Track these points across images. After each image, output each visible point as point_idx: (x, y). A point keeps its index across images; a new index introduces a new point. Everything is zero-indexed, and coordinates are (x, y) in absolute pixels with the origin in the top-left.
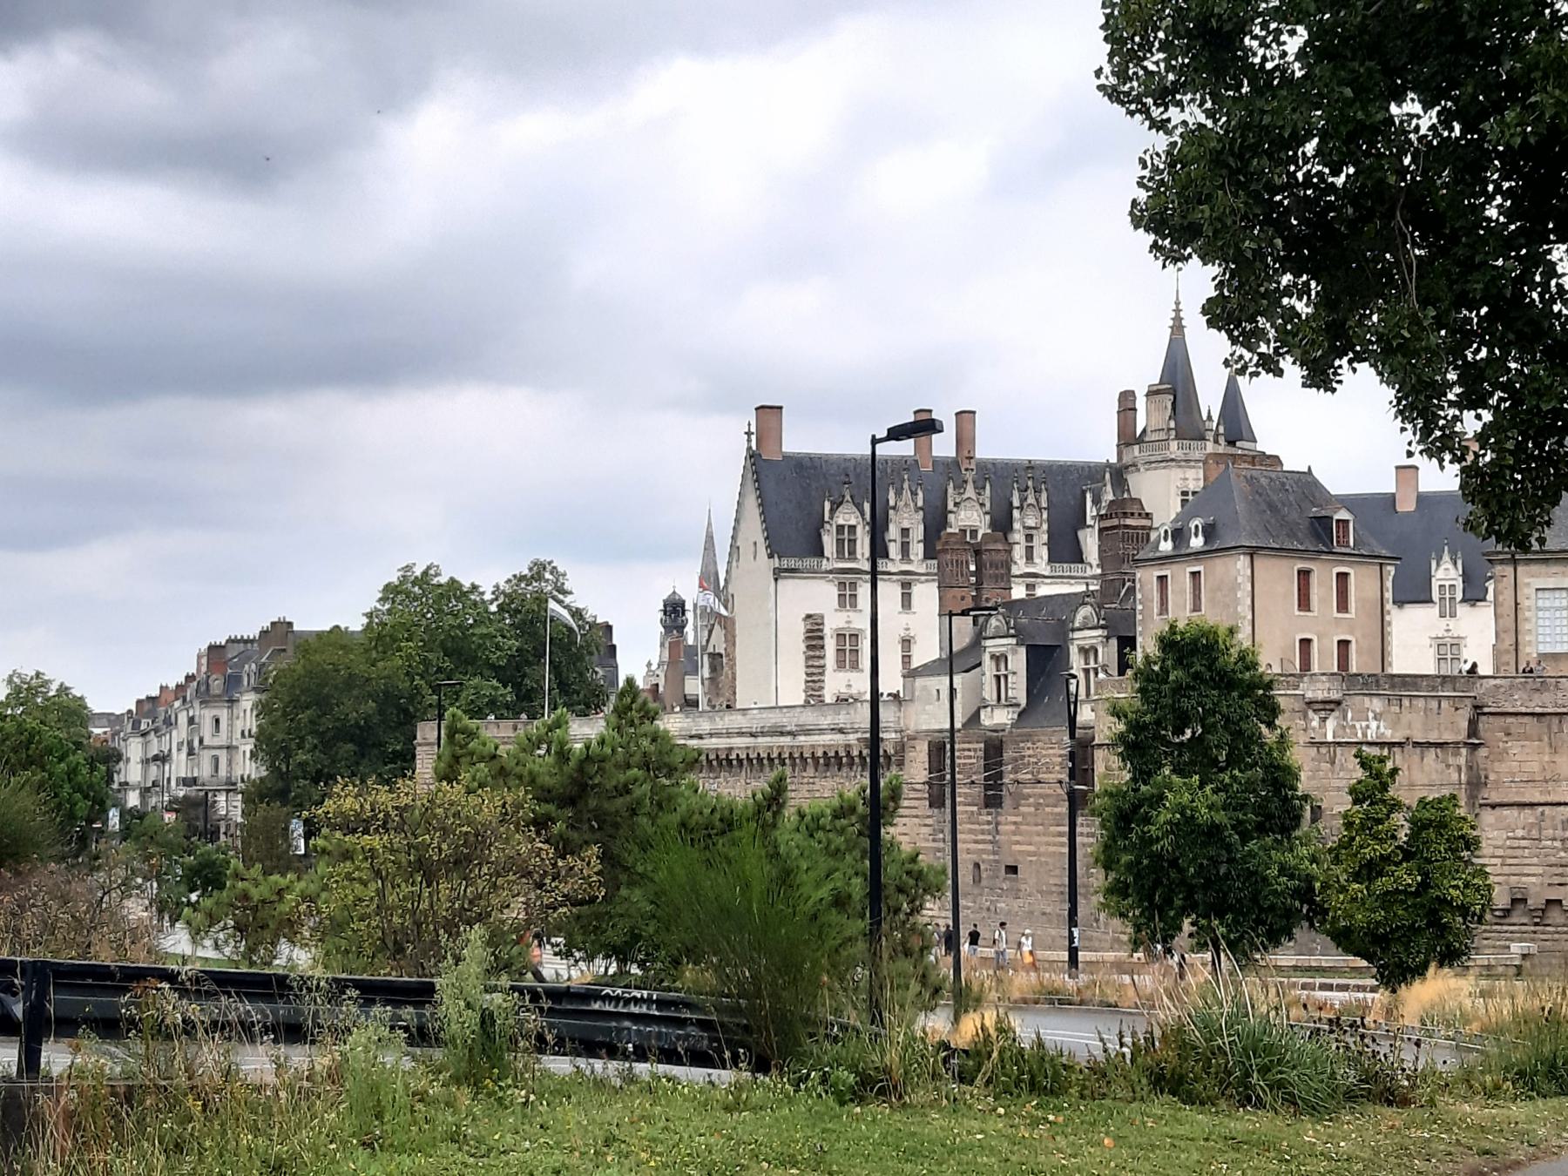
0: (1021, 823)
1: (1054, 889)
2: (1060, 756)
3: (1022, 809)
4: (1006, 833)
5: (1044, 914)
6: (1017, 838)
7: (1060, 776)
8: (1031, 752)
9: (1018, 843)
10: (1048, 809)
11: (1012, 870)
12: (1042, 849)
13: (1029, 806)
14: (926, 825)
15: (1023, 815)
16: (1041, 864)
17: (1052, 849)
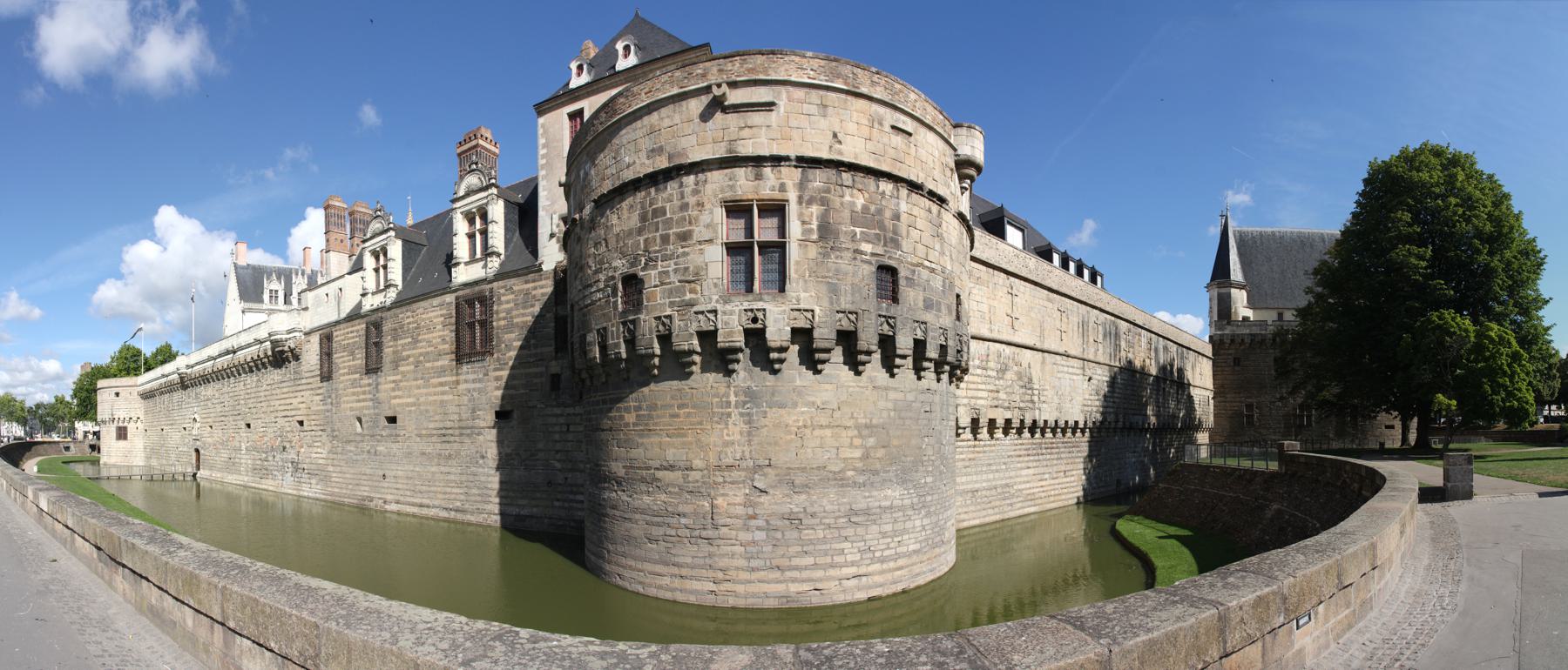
0: (401, 381)
1: (435, 432)
2: (441, 316)
3: (401, 369)
4: (386, 391)
5: (424, 454)
6: (397, 393)
7: (441, 333)
8: (411, 320)
9: (395, 397)
10: (428, 365)
11: (392, 420)
12: (422, 399)
13: (408, 365)
14: (318, 395)
15: (402, 373)
16: (421, 413)
17: (431, 398)
